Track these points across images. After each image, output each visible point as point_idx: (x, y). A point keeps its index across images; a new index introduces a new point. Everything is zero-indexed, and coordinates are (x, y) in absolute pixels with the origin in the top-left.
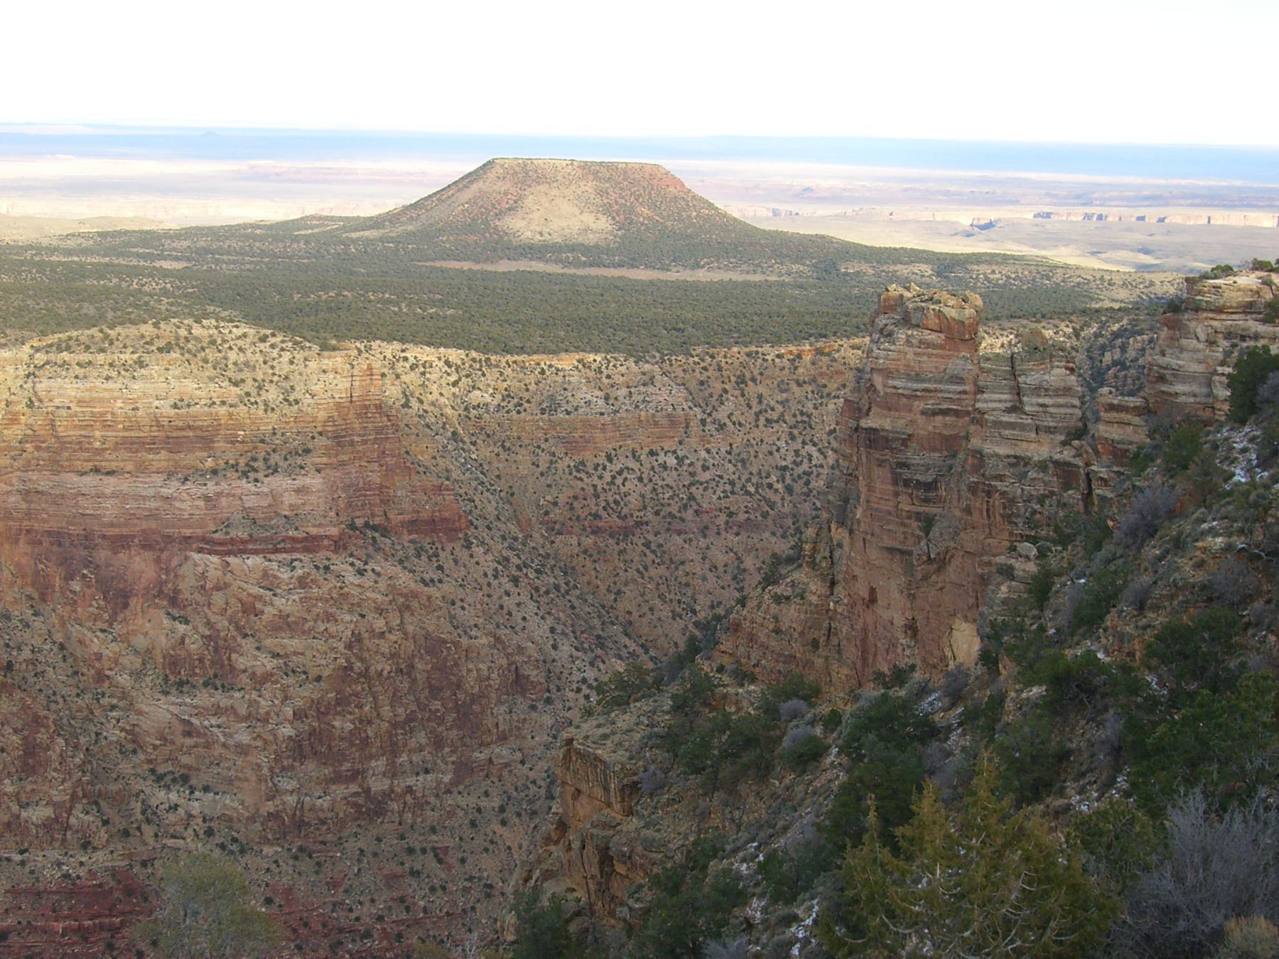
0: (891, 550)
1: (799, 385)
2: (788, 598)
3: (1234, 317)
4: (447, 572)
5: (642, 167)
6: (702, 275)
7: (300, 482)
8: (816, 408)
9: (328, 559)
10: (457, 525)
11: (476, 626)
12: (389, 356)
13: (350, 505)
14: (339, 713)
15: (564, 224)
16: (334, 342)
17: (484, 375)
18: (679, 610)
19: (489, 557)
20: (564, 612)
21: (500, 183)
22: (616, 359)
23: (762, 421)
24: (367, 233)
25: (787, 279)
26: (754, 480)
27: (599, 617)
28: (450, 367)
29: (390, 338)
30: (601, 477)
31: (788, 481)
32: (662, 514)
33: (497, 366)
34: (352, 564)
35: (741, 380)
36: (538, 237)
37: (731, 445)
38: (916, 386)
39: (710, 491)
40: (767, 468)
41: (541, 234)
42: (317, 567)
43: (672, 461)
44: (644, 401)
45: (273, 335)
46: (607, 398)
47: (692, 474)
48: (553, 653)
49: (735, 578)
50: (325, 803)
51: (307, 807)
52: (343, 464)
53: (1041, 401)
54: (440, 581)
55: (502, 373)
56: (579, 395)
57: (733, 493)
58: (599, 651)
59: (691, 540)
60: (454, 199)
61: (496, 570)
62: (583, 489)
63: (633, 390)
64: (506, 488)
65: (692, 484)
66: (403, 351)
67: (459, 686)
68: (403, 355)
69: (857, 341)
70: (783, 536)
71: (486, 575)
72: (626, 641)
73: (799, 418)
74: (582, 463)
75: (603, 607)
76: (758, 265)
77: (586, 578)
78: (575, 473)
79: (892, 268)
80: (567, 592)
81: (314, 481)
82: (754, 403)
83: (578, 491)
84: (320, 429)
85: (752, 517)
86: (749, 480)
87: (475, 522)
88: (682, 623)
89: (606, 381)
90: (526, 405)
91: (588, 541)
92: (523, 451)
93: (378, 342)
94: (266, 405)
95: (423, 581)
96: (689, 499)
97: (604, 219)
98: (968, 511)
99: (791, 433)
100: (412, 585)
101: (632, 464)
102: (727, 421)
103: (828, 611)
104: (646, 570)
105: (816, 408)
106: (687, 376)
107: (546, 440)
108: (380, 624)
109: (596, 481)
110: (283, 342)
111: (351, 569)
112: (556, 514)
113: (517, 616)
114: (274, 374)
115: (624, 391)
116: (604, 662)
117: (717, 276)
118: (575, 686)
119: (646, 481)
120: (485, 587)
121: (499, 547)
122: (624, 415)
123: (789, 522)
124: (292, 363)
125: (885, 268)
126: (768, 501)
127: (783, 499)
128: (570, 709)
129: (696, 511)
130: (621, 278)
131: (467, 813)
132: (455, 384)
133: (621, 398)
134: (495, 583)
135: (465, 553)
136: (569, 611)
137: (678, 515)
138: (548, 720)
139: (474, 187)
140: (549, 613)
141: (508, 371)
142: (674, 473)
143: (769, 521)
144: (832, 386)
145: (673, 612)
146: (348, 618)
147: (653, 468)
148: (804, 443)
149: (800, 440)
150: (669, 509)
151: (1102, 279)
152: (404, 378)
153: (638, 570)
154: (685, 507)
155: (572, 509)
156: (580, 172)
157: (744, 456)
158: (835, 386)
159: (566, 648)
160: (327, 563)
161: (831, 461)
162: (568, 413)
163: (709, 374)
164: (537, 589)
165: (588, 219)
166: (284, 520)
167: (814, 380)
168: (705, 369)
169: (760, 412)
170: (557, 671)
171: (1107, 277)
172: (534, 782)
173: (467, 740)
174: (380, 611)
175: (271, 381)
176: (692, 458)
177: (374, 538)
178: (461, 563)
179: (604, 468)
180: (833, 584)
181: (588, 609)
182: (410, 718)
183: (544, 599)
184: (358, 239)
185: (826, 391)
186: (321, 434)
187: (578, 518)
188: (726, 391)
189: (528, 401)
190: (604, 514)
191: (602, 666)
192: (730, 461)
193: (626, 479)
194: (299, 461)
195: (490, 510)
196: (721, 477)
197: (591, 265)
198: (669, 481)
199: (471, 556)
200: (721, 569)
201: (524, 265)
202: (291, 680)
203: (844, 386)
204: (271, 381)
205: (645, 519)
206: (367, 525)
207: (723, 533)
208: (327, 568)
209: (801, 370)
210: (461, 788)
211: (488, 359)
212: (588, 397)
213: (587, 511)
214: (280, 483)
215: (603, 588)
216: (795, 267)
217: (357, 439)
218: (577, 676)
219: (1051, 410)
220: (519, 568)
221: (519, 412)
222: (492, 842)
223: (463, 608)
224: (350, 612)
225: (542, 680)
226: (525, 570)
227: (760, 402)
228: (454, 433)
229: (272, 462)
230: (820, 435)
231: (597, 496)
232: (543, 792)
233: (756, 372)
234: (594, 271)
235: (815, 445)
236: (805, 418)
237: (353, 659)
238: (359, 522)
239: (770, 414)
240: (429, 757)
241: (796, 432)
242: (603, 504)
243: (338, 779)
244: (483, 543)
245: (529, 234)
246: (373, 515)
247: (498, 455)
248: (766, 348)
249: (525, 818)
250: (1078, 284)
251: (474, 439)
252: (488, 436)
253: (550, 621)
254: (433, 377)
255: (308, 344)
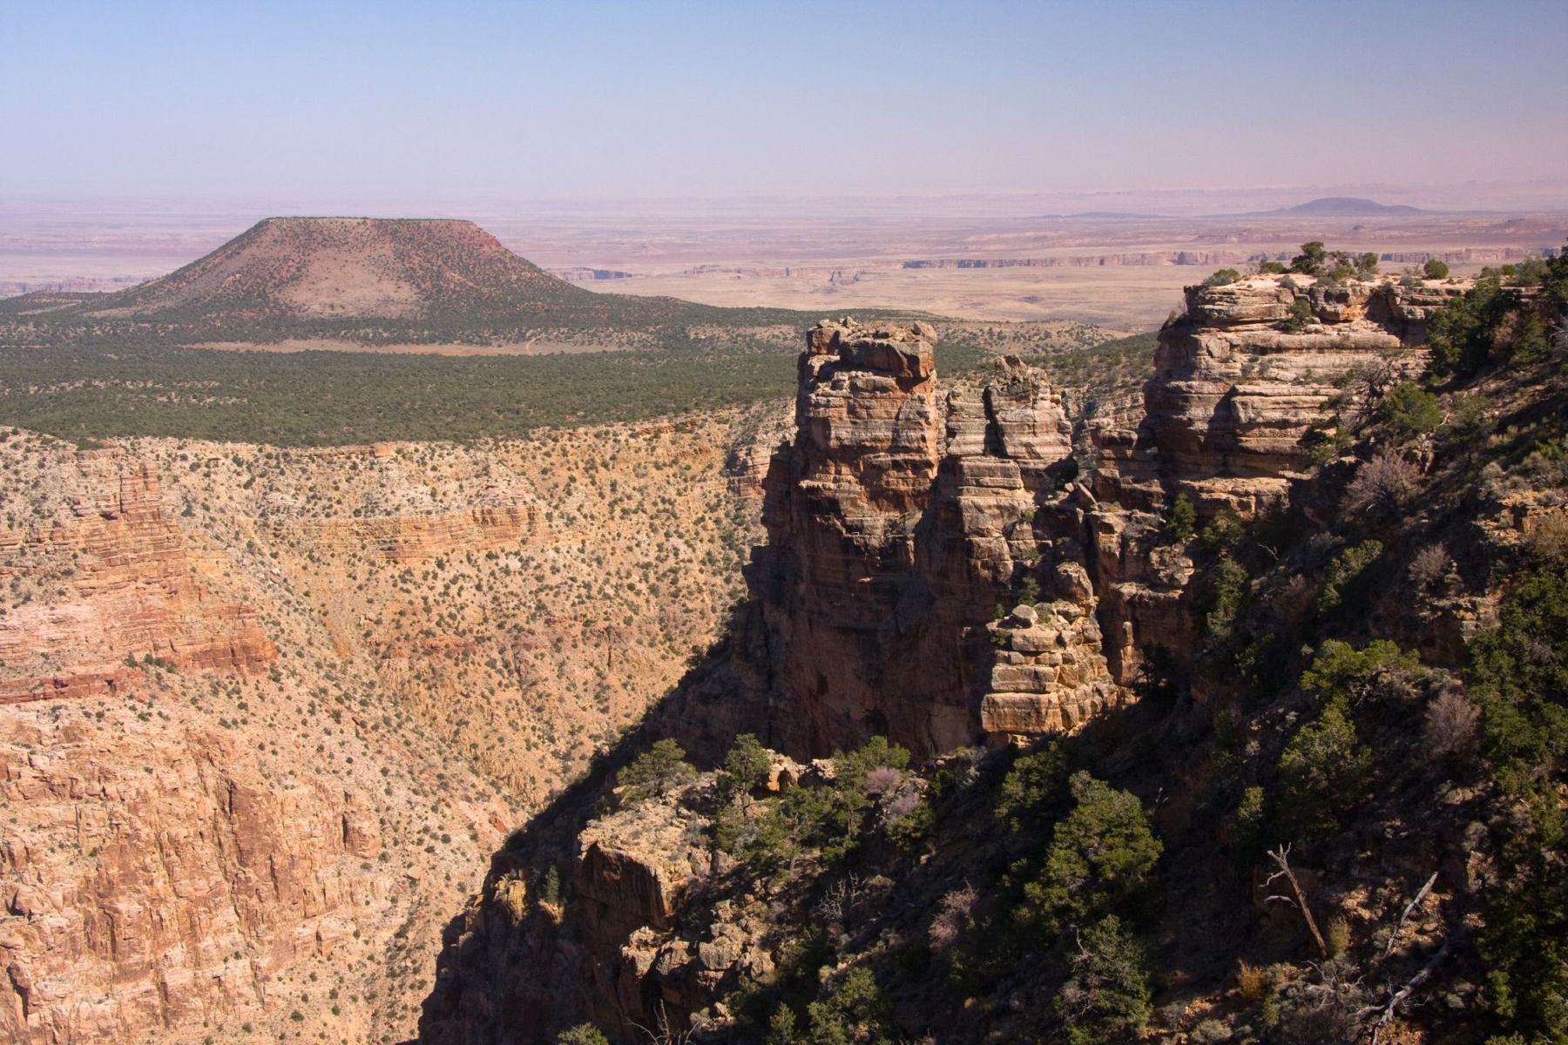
0: (844, 630)
1: (658, 467)
2: (717, 697)
3: (1254, 326)
4: (252, 710)
5: (449, 223)
6: (529, 349)
7: (60, 611)
8: (679, 494)
9: (101, 704)
10: (261, 653)
11: (291, 773)
12: (163, 454)
13: (126, 635)
14: (123, 893)
15: (358, 293)
16: (93, 440)
17: (282, 473)
18: (534, 739)
19: (303, 689)
20: (397, 749)
21: (279, 247)
22: (442, 448)
23: (618, 512)
24: (114, 312)
25: (627, 348)
26: (614, 581)
27: (440, 753)
28: (240, 464)
29: (162, 434)
30: (431, 588)
31: (652, 579)
32: (507, 626)
33: (298, 462)
34: (133, 708)
35: (591, 466)
36: (328, 310)
37: (583, 542)
38: (863, 436)
39: (562, 596)
40: (627, 566)
41: (332, 306)
42: (87, 715)
43: (515, 564)
44: (478, 495)
45: (15, 433)
46: (433, 494)
47: (539, 579)
48: (387, 799)
49: (597, 697)
50: (108, 1007)
51: (83, 1015)
52: (116, 587)
53: (1025, 439)
54: (245, 722)
55: (304, 471)
56: (399, 493)
57: (589, 597)
58: (442, 793)
59: (543, 655)
60: (221, 268)
61: (312, 705)
62: (411, 603)
63: (464, 483)
64: (317, 606)
65: (541, 590)
66: (180, 448)
67: (274, 848)
68: (180, 453)
69: (724, 414)
70: (651, 645)
71: (299, 711)
72: (473, 778)
73: (661, 506)
74: (409, 572)
75: (443, 740)
76: (594, 335)
77: (422, 708)
78: (400, 585)
79: (749, 331)
80: (399, 726)
81: (80, 610)
82: (607, 490)
83: (405, 605)
84: (82, 545)
85: (614, 624)
86: (607, 582)
87: (284, 649)
88: (537, 753)
89: (431, 474)
90: (336, 506)
91: (423, 664)
92: (335, 561)
93: (148, 439)
94: (10, 519)
95: (223, 723)
96: (538, 608)
97: (406, 287)
98: (944, 574)
99: (651, 525)
100: (211, 729)
101: (467, 569)
102: (577, 514)
103: (767, 708)
104: (492, 692)
105: (679, 494)
106: (527, 464)
107: (363, 547)
108: (171, 779)
109: (425, 591)
110: (28, 441)
111: (132, 714)
112: (379, 634)
113: (341, 758)
114: (18, 481)
115: (454, 485)
116: (448, 806)
117: (545, 349)
118: (416, 837)
119: (485, 589)
120: (300, 726)
121: (315, 678)
122: (456, 513)
123: (656, 627)
124: (41, 466)
125: (741, 331)
126: (630, 605)
127: (648, 601)
128: (410, 865)
129: (547, 622)
130: (433, 356)
131: (290, 1003)
132: (247, 485)
133: (450, 494)
134: (311, 720)
135: (274, 686)
136: (404, 749)
137: (526, 627)
138: (385, 883)
139: (246, 253)
140: (379, 752)
141: (313, 467)
142: (519, 579)
143: (634, 628)
144: (697, 468)
145: (527, 741)
146: (131, 774)
147: (492, 574)
148: (667, 535)
149: (662, 532)
150: (513, 621)
151: (990, 332)
152: (183, 480)
153: (483, 696)
154: (533, 617)
155: (399, 627)
156: (375, 232)
157: (600, 553)
158: (701, 467)
159: (402, 793)
160: (100, 709)
161: (701, 555)
162: (388, 514)
163: (552, 460)
164: (363, 725)
165: (388, 288)
166: (42, 660)
167: (675, 462)
168: (547, 454)
169: (615, 502)
170: (394, 821)
171: (996, 330)
172: (371, 958)
173: (287, 913)
174: (172, 763)
175: (16, 490)
176: (539, 559)
177: (159, 676)
178: (268, 698)
179: (435, 576)
180: (771, 676)
181: (425, 745)
182: (215, 892)
183: (374, 735)
184: (103, 319)
185: (689, 474)
186: (84, 551)
187: (407, 638)
188: (573, 479)
189: (339, 502)
190: (439, 631)
191: (447, 811)
192: (583, 561)
193: (461, 588)
194: (58, 585)
195: (300, 635)
196: (573, 579)
197: (395, 342)
198: (513, 588)
199: (281, 689)
200: (580, 687)
201: (314, 344)
202: (59, 857)
203: (710, 467)
204: (16, 490)
205: (488, 634)
206: (148, 660)
207: (581, 645)
208: (100, 715)
209: (659, 451)
210: (281, 973)
211: (286, 455)
212: (412, 494)
213: (417, 628)
214: (35, 613)
215: (441, 718)
216: (636, 336)
217: (131, 555)
218: (418, 825)
219: (1038, 449)
220: (339, 700)
221: (328, 516)
222: (322, 1036)
223: (274, 753)
224: (133, 766)
225: (377, 834)
226: (347, 703)
227: (614, 490)
228: (250, 545)
229: (23, 588)
230: (687, 523)
231: (428, 610)
232: (384, 970)
233: (607, 457)
234: (401, 349)
235: (681, 536)
236: (668, 506)
237: (139, 825)
238: (139, 657)
239: (626, 504)
240: (239, 937)
241: (657, 522)
242: (437, 619)
243: (125, 975)
244: (293, 674)
245: (316, 307)
246: (156, 648)
247: (305, 568)
248: (618, 427)
249: (361, 1002)
250: (964, 339)
251: (274, 550)
252: (292, 545)
253: (381, 762)
254: (220, 478)
255: (61, 443)
